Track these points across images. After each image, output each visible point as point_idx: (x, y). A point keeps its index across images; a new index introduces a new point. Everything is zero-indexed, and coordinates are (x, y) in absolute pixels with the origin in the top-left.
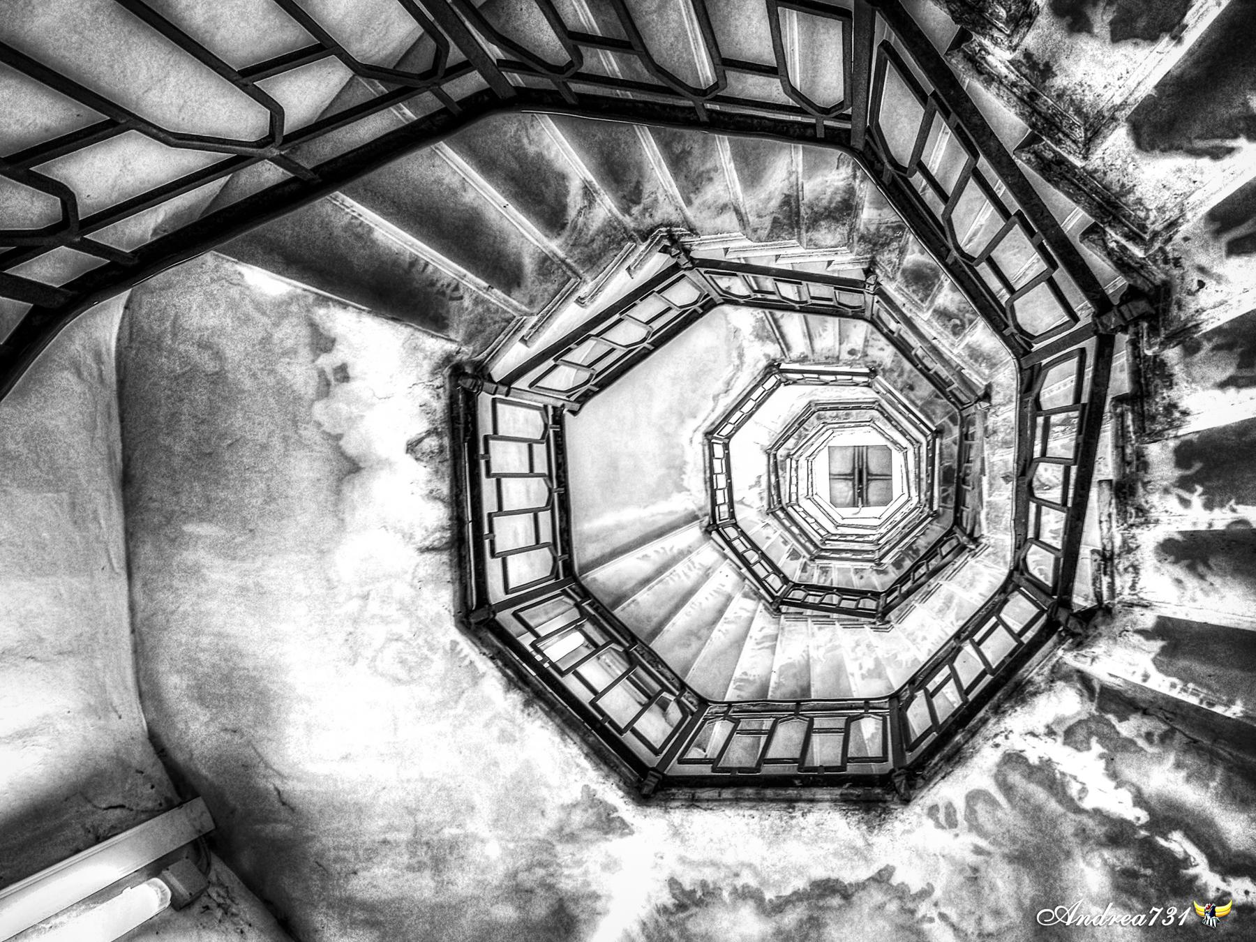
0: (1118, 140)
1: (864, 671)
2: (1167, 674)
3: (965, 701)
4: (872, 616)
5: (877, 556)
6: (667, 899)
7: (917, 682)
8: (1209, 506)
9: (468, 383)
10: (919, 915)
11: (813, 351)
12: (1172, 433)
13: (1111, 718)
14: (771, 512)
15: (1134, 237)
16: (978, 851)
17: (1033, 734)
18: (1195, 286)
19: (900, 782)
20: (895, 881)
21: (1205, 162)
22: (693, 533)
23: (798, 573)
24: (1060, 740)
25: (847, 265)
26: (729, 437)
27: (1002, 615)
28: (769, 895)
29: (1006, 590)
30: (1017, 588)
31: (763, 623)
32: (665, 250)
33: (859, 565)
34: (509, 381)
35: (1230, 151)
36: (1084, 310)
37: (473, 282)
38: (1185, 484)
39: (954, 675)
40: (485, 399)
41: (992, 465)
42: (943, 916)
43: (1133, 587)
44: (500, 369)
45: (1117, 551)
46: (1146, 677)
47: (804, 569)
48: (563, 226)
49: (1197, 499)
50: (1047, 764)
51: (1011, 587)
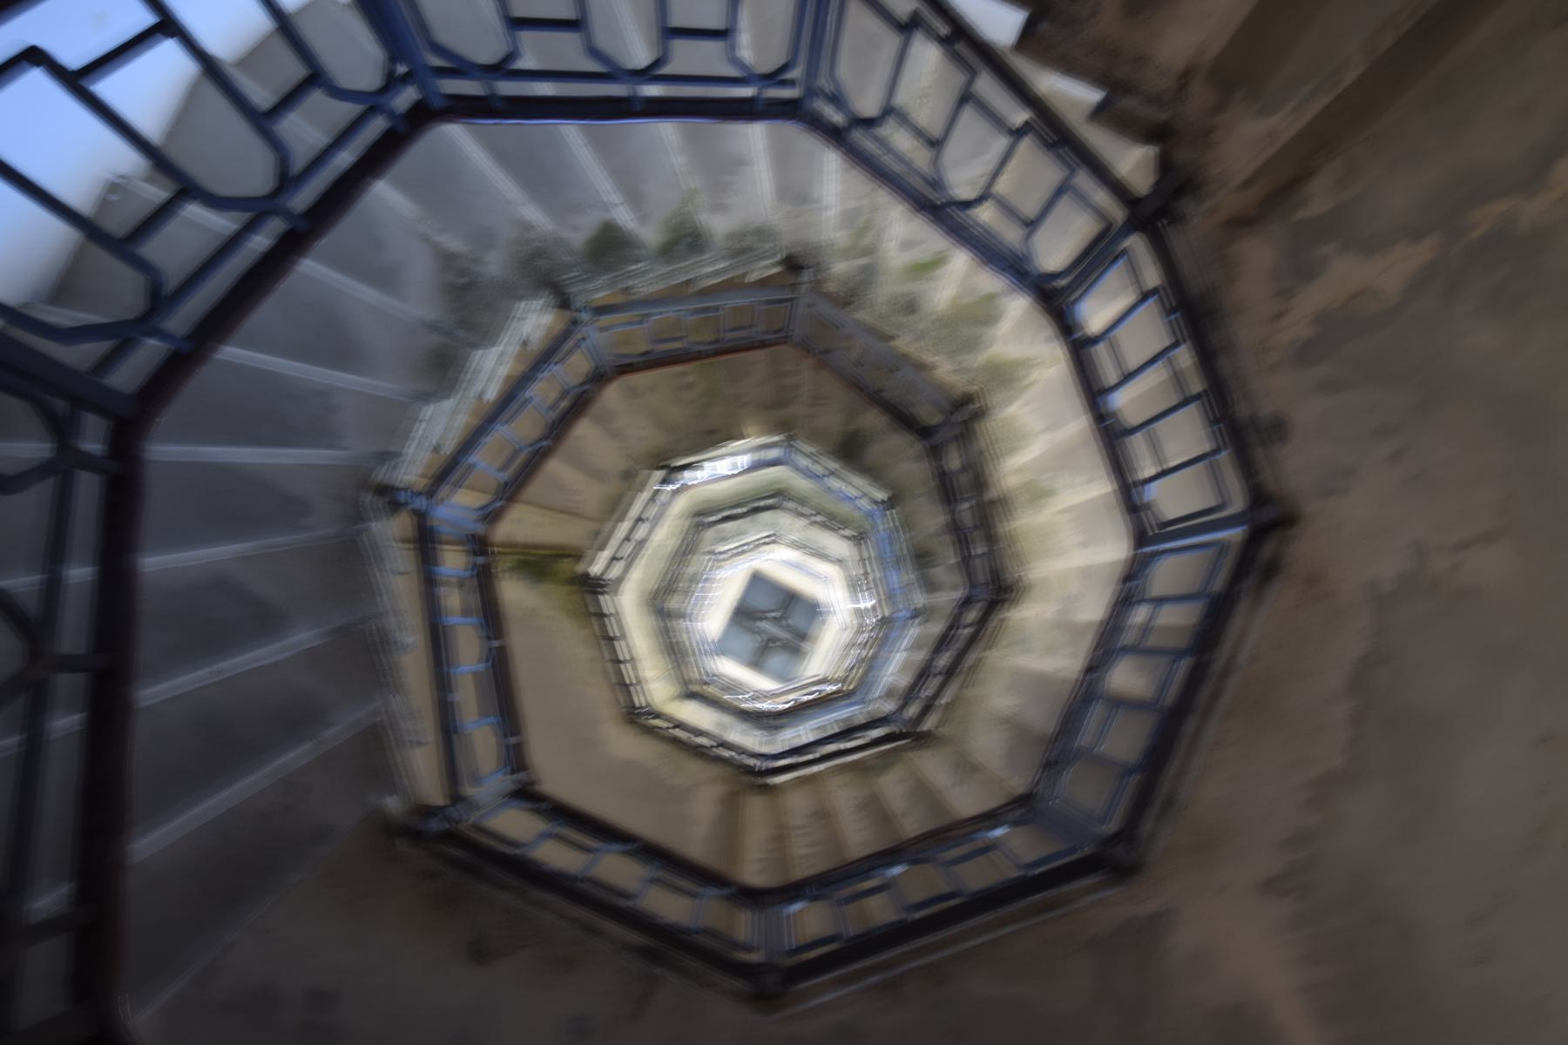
13: (1301, 214)
17: (1280, 315)
22: (755, 806)
25: (534, 321)
37: (295, 757)
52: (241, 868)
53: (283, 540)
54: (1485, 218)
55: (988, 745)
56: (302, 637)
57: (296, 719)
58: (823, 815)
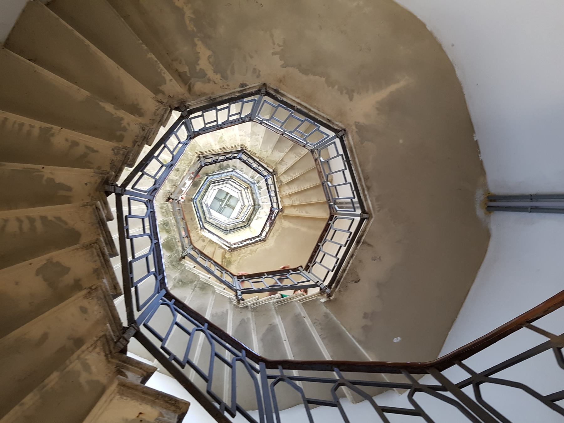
0: (85, 240)
1: (257, 136)
2: (164, 78)
3: (230, 105)
4: (245, 152)
5: (233, 173)
6: (356, 96)
7: (242, 121)
8: (122, 119)
9: (328, 290)
10: (281, 48)
11: (215, 248)
12: (120, 146)
13: (188, 75)
14: (259, 205)
15: (97, 208)
16: (251, 57)
17: (215, 83)
18: (88, 184)
19: (263, 91)
20: (282, 62)
21: (64, 218)
22: (287, 212)
23: (261, 182)
24: (207, 76)
25: (188, 264)
26: (258, 237)
27: (203, 126)
28: (323, 79)
29: (198, 133)
30: (194, 132)
31: (281, 169)
32: (243, 300)
33: (241, 173)
34: (315, 286)
35: (55, 217)
36: (125, 198)
37: (308, 322)
38: (125, 129)
39: (229, 116)
40: (326, 283)
41: (180, 177)
42: (274, 44)
43: (159, 108)
44: (317, 290)
45: (157, 123)
46: (171, 80)
47: (258, 182)
48: (271, 325)
49: (124, 123)
50: (215, 72)
51: (196, 133)
52: (333, 334)
53: (252, 326)
54: (191, 27)
55: (278, 156)
56: (278, 320)
57: (298, 322)
58: (290, 195)
